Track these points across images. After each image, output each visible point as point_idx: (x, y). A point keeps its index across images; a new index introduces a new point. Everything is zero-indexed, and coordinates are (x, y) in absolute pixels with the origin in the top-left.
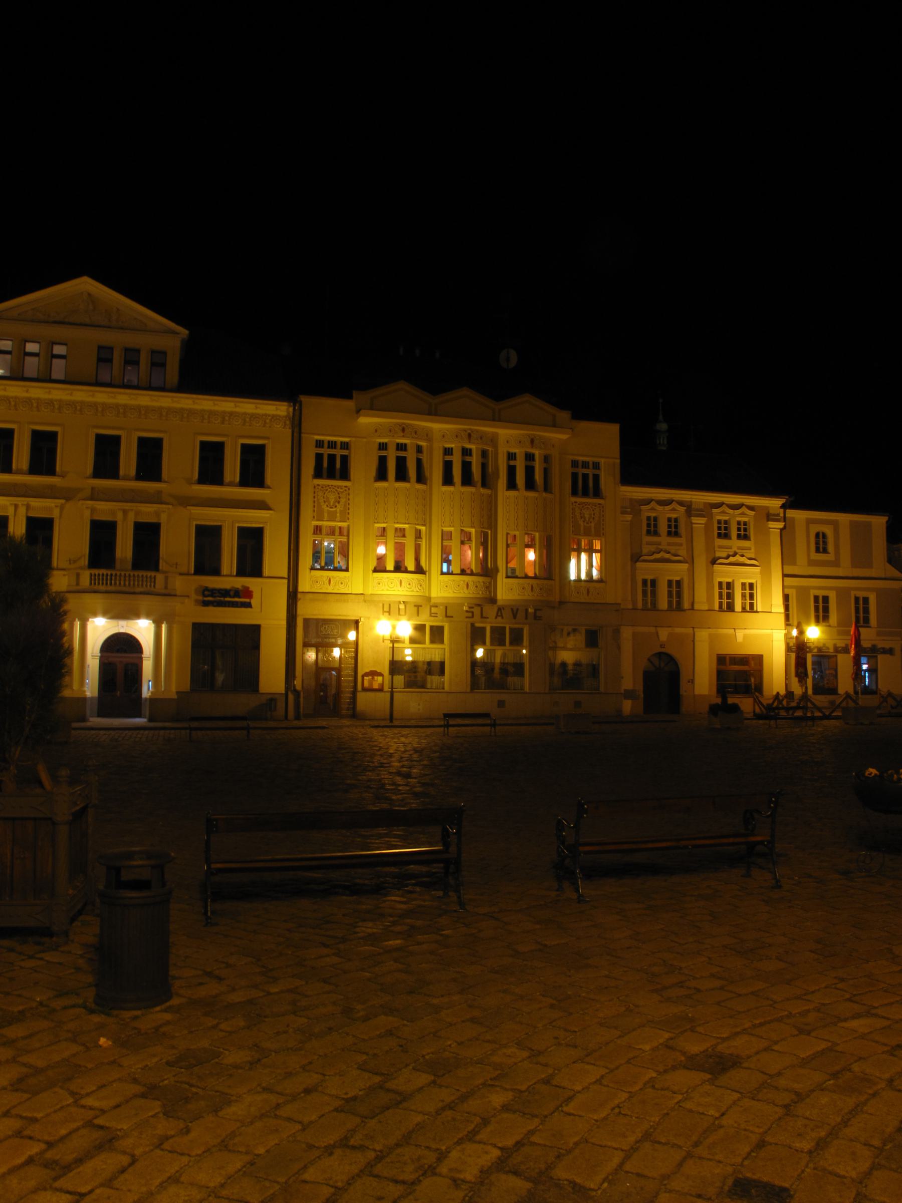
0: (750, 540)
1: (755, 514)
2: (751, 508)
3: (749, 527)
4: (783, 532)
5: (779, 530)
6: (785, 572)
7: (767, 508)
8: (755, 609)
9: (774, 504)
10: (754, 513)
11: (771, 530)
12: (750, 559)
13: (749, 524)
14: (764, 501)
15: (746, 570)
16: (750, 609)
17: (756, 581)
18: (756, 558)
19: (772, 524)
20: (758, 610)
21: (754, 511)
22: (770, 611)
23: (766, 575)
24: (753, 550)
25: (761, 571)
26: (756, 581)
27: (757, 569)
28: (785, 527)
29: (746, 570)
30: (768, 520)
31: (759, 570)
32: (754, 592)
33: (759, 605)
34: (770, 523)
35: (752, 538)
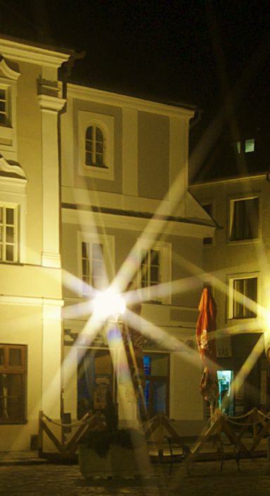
0: (11, 127)
1: (20, 77)
2: (14, 66)
3: (10, 101)
4: (62, 116)
5: (56, 113)
6: (64, 201)
7: (40, 67)
8: (15, 260)
9: (50, 60)
10: (19, 74)
11: (43, 110)
12: (11, 163)
13: (10, 93)
14: (39, 56)
15: (9, 184)
16: (7, 259)
17: (19, 207)
18: (21, 164)
19: (46, 101)
20: (21, 262)
21: (18, 72)
22: (39, 264)
23: (35, 195)
24: (15, 148)
25: (26, 188)
26: (19, 207)
27: (21, 184)
28: (64, 110)
29: (9, 184)
30: (39, 93)
31: (24, 186)
32: (15, 226)
33: (24, 253)
34: (43, 97)
35: (14, 124)
